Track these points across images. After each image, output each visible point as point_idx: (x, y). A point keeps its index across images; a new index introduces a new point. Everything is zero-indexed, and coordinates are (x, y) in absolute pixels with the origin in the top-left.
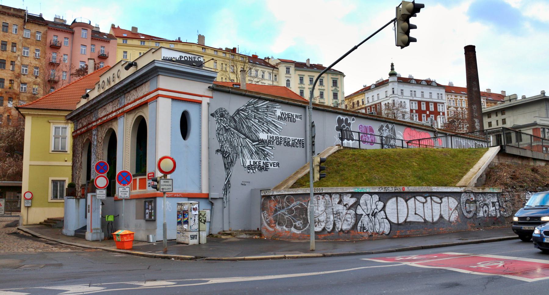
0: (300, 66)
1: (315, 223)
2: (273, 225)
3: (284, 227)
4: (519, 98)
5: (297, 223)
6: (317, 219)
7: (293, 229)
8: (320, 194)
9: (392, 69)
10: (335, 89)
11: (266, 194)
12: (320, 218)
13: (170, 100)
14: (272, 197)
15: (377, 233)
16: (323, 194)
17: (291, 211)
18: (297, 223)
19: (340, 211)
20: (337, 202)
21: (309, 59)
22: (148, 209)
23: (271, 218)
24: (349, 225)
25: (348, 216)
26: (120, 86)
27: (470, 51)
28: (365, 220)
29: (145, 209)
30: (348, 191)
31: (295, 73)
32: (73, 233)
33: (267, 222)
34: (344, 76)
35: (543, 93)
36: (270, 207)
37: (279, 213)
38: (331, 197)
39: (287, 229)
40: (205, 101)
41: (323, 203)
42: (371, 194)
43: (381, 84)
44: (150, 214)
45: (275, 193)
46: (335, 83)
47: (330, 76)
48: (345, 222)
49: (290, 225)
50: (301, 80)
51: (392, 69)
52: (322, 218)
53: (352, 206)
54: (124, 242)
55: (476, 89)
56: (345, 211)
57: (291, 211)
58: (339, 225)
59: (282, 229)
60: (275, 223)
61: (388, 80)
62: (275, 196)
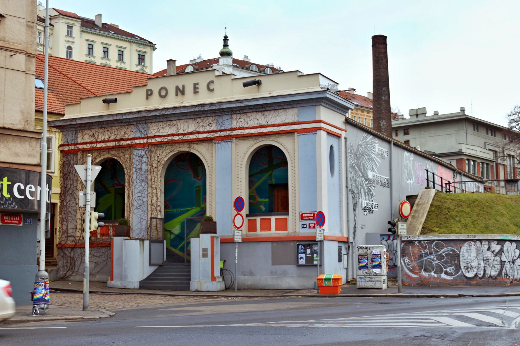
0: (88, 25)
1: (467, 269)
2: (417, 271)
3: (433, 273)
4: (430, 113)
5: (448, 269)
6: (469, 265)
7: (443, 276)
8: (472, 240)
9: (226, 46)
10: (142, 69)
11: (409, 239)
12: (472, 264)
13: (326, 133)
14: (416, 243)
15: (516, 280)
16: (475, 241)
17: (440, 257)
18: (448, 269)
19: (489, 258)
20: (486, 249)
21: (100, 15)
22: (305, 253)
23: (415, 264)
24: (496, 271)
25: (495, 262)
26: (234, 105)
27: (379, 43)
28: (507, 266)
29: (298, 253)
30: (496, 238)
31: (81, 37)
32: (137, 285)
33: (409, 269)
34: (154, 49)
35: (463, 110)
36: (413, 253)
37: (425, 258)
38: (481, 243)
39: (436, 276)
40: (343, 134)
41: (475, 250)
42: (511, 241)
43: (203, 66)
44: (310, 260)
45: (421, 238)
46: (141, 59)
47: (135, 47)
48: (493, 268)
49: (439, 271)
50: (91, 49)
51: (226, 46)
52: (474, 264)
53: (498, 253)
54: (337, 286)
55: (387, 98)
56: (493, 258)
57: (440, 257)
58: (488, 272)
59: (429, 275)
60: (420, 269)
61: (216, 61)
62: (420, 241)
